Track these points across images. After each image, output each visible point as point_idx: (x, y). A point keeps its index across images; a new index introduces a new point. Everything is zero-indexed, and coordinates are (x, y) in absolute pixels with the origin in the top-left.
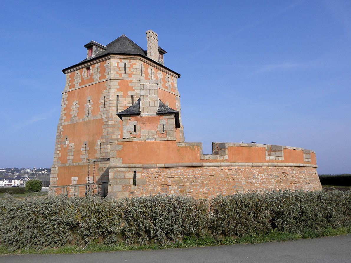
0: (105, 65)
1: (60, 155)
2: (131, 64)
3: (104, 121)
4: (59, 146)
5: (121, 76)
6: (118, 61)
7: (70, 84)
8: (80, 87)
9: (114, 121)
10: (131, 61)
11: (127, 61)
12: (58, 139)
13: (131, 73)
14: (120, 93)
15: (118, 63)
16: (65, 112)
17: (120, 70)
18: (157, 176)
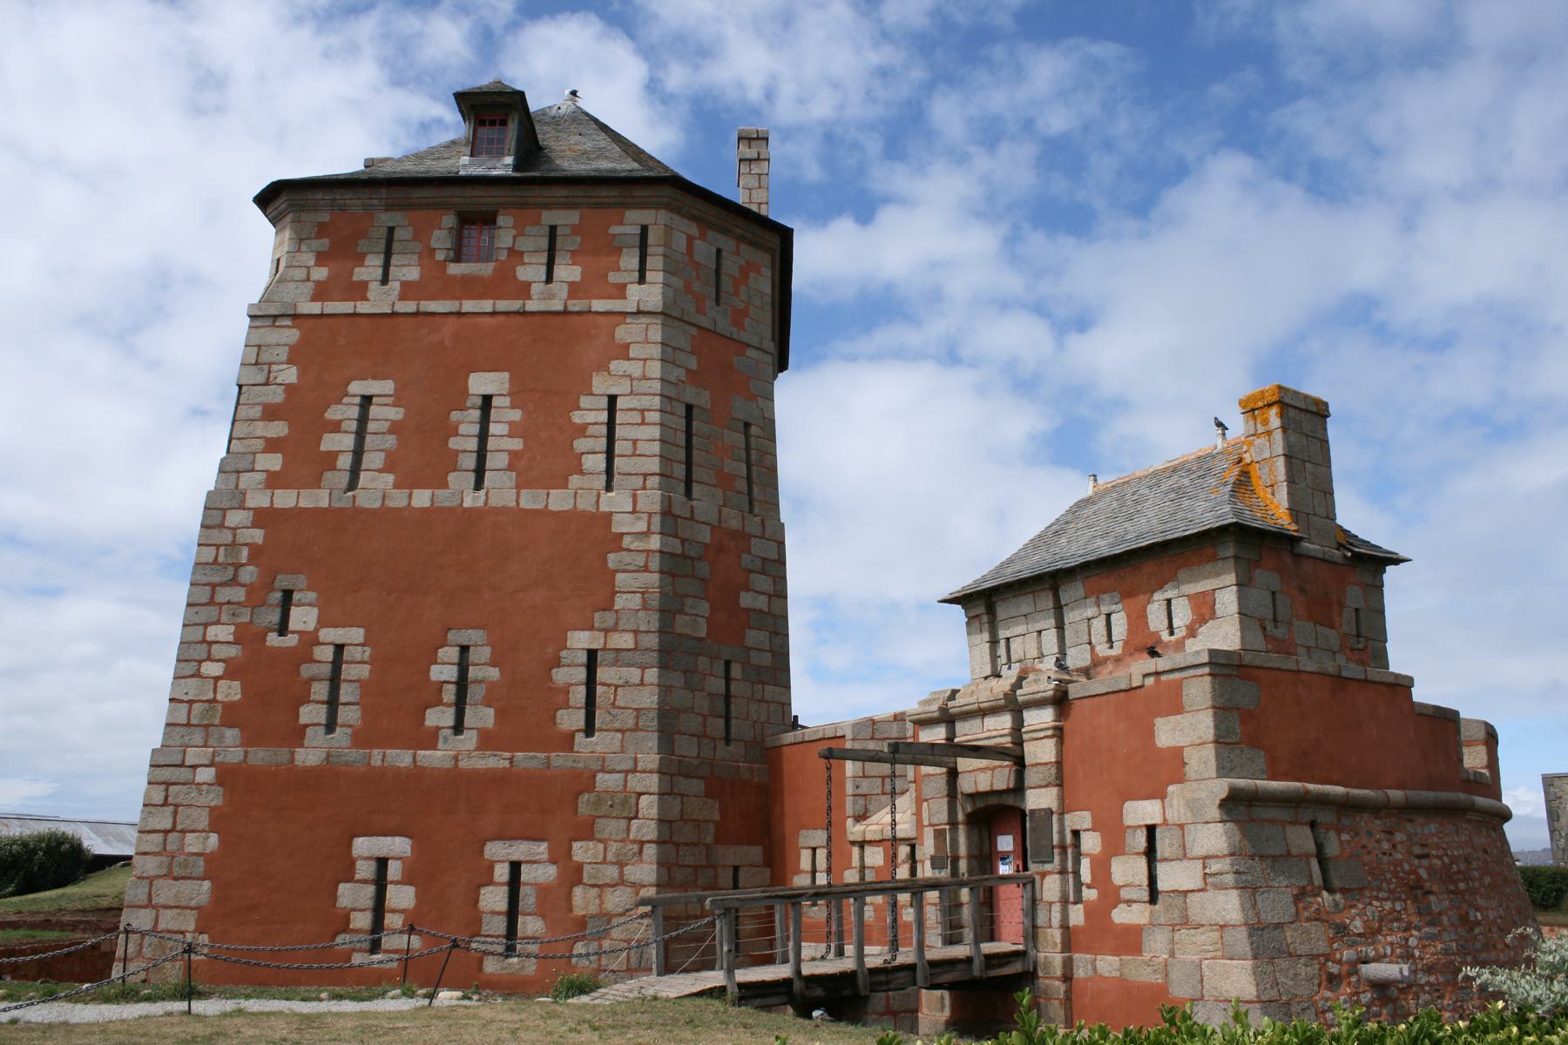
0: (614, 230)
1: (231, 691)
2: (743, 263)
3: (624, 531)
4: (223, 632)
5: (700, 311)
6: (694, 230)
7: (321, 273)
8: (409, 307)
9: (683, 541)
10: (744, 248)
11: (727, 244)
12: (213, 586)
13: (741, 306)
14: (702, 399)
15: (690, 239)
16: (279, 429)
17: (698, 278)
18: (1386, 846)
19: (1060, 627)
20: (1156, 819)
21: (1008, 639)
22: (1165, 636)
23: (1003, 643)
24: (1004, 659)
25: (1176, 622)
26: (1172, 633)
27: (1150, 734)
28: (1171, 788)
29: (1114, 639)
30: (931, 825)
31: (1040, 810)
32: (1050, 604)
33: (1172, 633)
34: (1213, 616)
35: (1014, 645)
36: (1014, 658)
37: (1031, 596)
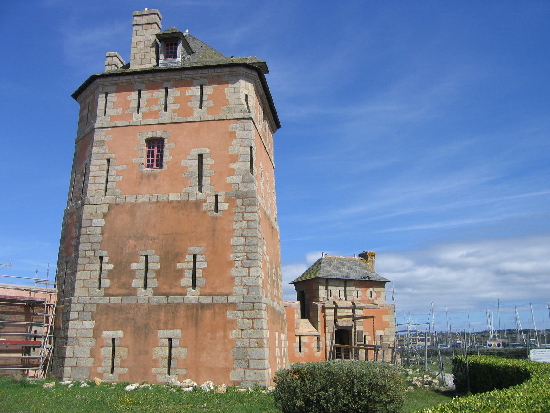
19: (345, 291)
20: (383, 334)
21: (331, 290)
23: (329, 291)
24: (329, 295)
25: (372, 296)
26: (371, 298)
27: (381, 318)
28: (386, 329)
29: (358, 296)
30: (329, 332)
31: (360, 331)
32: (344, 285)
33: (371, 298)
34: (380, 296)
35: (332, 292)
36: (332, 294)
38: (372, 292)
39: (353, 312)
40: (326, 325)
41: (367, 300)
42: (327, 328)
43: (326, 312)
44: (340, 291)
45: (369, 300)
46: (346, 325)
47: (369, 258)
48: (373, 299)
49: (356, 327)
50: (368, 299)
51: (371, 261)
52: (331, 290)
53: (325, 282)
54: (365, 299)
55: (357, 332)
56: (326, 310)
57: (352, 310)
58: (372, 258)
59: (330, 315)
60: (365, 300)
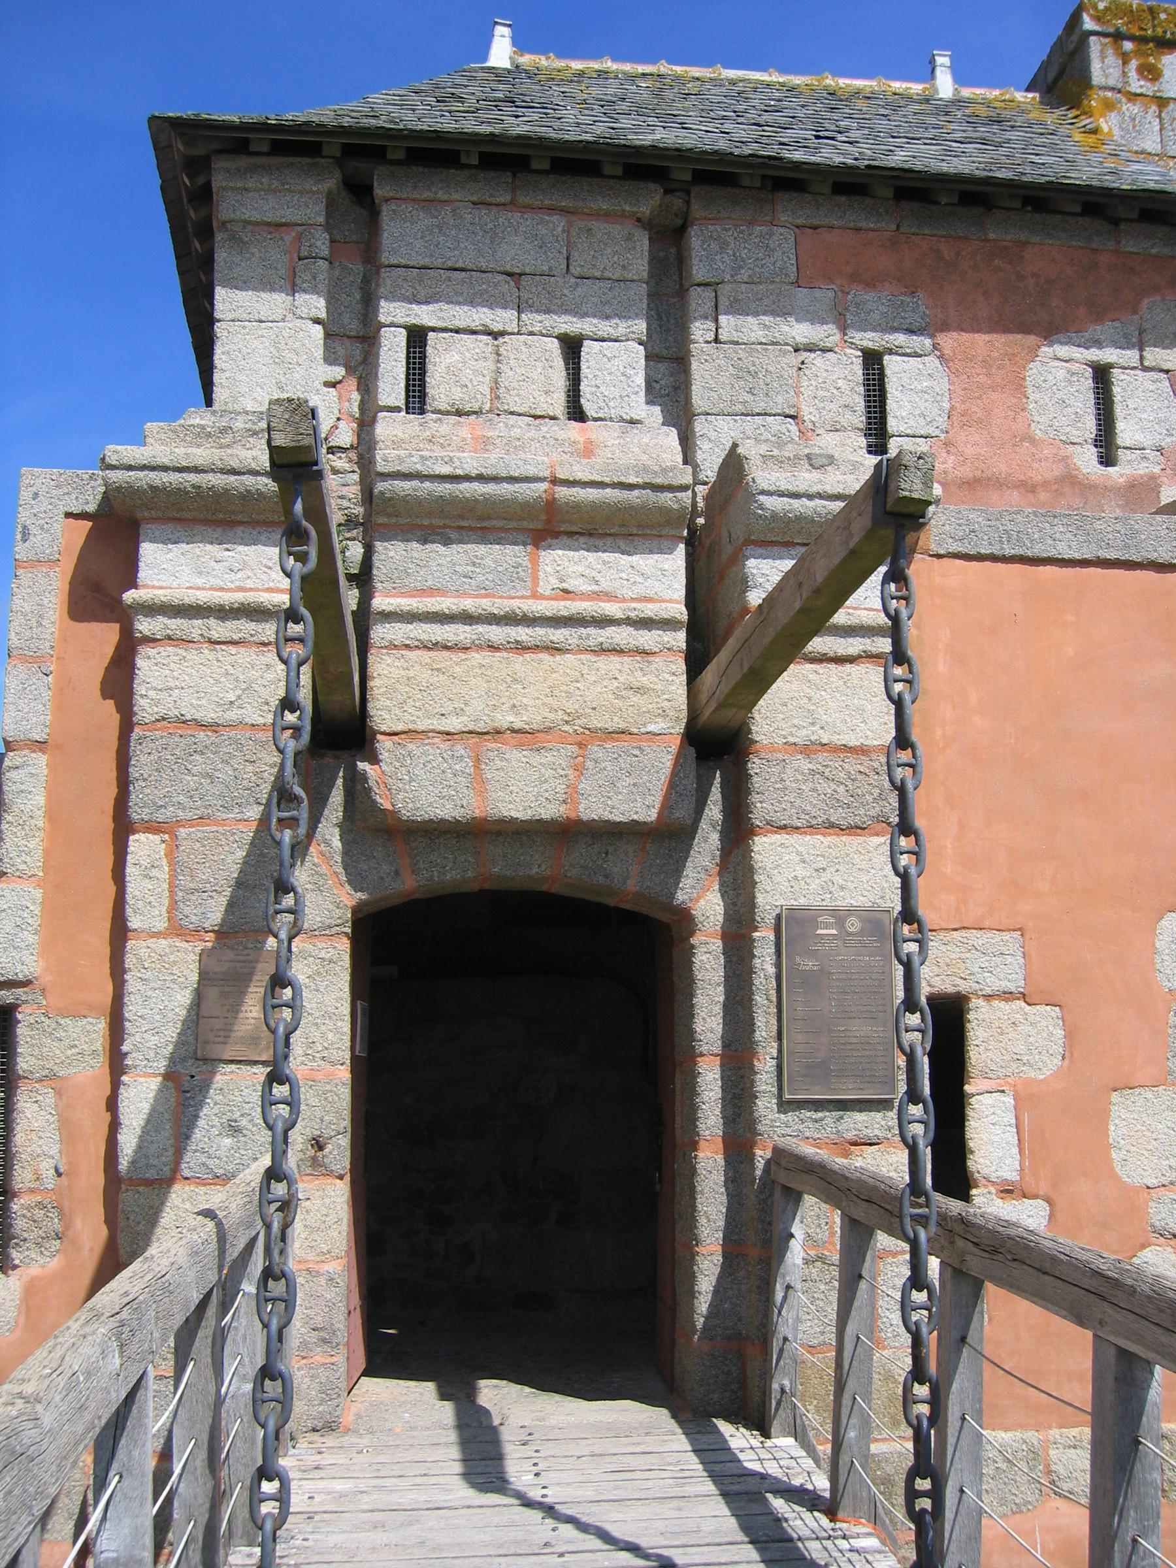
21: (417, 338)
22: (1087, 459)
25: (1126, 432)
26: (1107, 459)
29: (892, 425)
30: (177, 929)
31: (840, 916)
32: (640, 266)
37: (558, 223)
38: (1121, 383)
39: (691, 601)
40: (137, 812)
41: (1029, 488)
42: (142, 846)
43: (144, 574)
44: (572, 347)
45: (1071, 480)
46: (550, 811)
47: (1112, 60)
48: (1143, 469)
49: (764, 848)
50: (1058, 470)
51: (1133, 97)
52: (417, 338)
53: (316, 212)
54: (1000, 467)
55: (764, 936)
56: (148, 550)
57: (676, 561)
58: (1151, 73)
59: (220, 629)
60: (1000, 484)
